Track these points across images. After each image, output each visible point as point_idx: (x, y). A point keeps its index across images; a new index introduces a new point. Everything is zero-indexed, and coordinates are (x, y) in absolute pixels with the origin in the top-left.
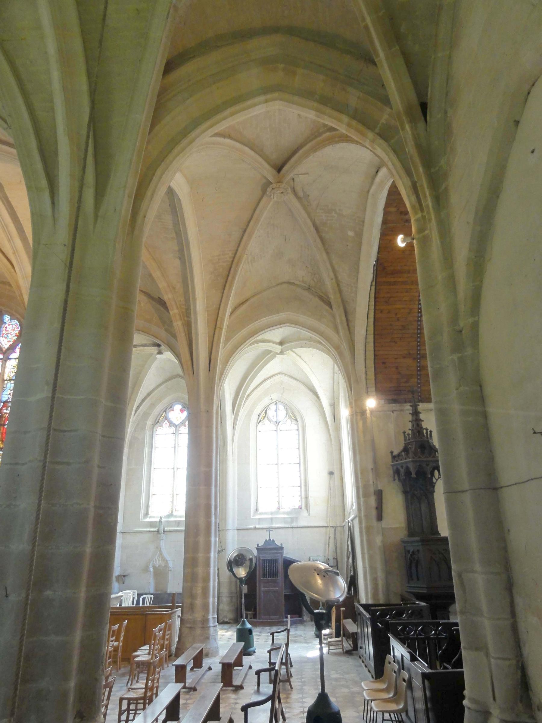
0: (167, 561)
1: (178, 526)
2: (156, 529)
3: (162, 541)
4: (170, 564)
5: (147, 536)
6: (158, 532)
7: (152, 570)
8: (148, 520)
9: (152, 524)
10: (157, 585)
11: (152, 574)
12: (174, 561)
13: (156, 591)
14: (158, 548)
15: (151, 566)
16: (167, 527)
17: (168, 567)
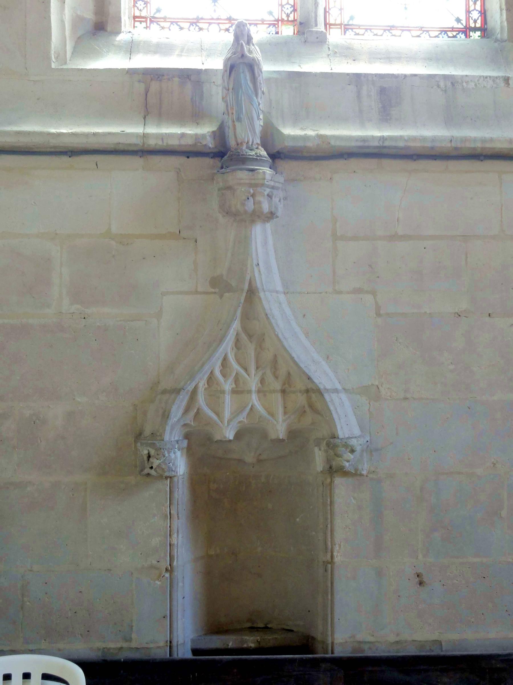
0: (313, 391)
1: (385, 116)
2: (202, 131)
3: (260, 234)
4: (347, 423)
5: (127, 181)
6: (223, 154)
7: (180, 464)
8: (110, 61)
9: (158, 91)
10: (216, 577)
11: (182, 493)
12: (372, 393)
13: (215, 628)
14: (236, 292)
15: (173, 434)
16: (296, 120)
17: (332, 443)
